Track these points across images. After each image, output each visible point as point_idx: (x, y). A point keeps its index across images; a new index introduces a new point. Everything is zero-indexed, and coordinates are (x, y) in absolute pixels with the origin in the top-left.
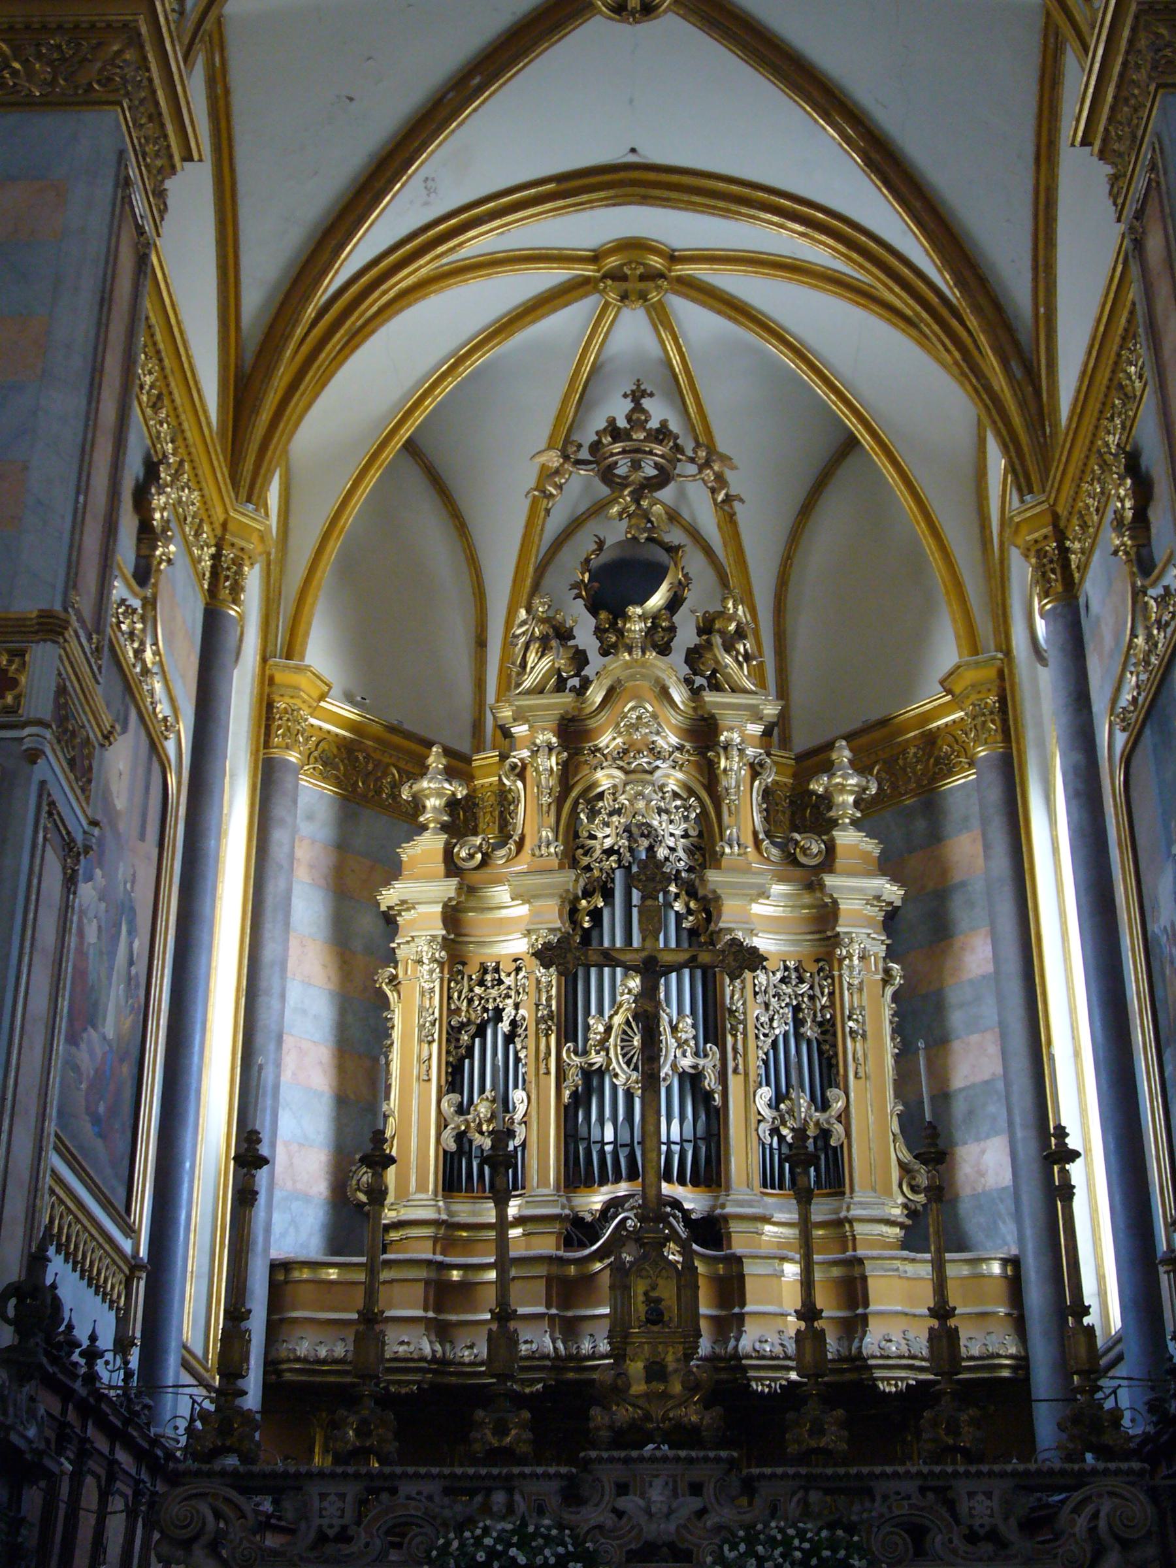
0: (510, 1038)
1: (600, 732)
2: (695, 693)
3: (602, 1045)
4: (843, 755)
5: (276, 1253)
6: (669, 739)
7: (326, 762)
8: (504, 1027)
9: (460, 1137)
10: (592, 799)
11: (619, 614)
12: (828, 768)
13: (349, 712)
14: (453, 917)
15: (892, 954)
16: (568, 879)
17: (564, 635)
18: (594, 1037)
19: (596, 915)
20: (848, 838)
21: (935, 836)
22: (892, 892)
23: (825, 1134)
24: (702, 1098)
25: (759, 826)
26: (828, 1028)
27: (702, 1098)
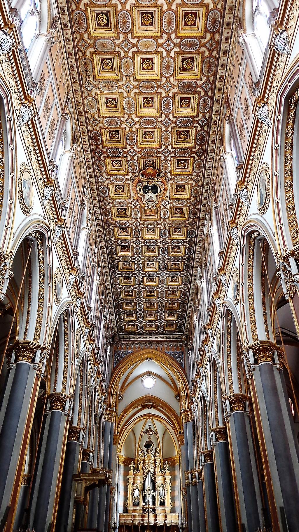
0: (138, 491)
1: (146, 460)
2: (154, 458)
3: (146, 492)
4: (167, 463)
5: (119, 513)
6: (152, 461)
7: (123, 462)
8: (138, 489)
9: (134, 500)
10: (145, 467)
11: (148, 449)
12: (165, 464)
13: (124, 457)
14: (134, 479)
15: (170, 482)
16: (144, 476)
17: (143, 451)
18: (145, 491)
19: (145, 479)
20: (167, 471)
21: (174, 470)
22: (170, 477)
23: (164, 500)
24: (154, 497)
25: (159, 470)
26: (165, 490)
27: (154, 497)
